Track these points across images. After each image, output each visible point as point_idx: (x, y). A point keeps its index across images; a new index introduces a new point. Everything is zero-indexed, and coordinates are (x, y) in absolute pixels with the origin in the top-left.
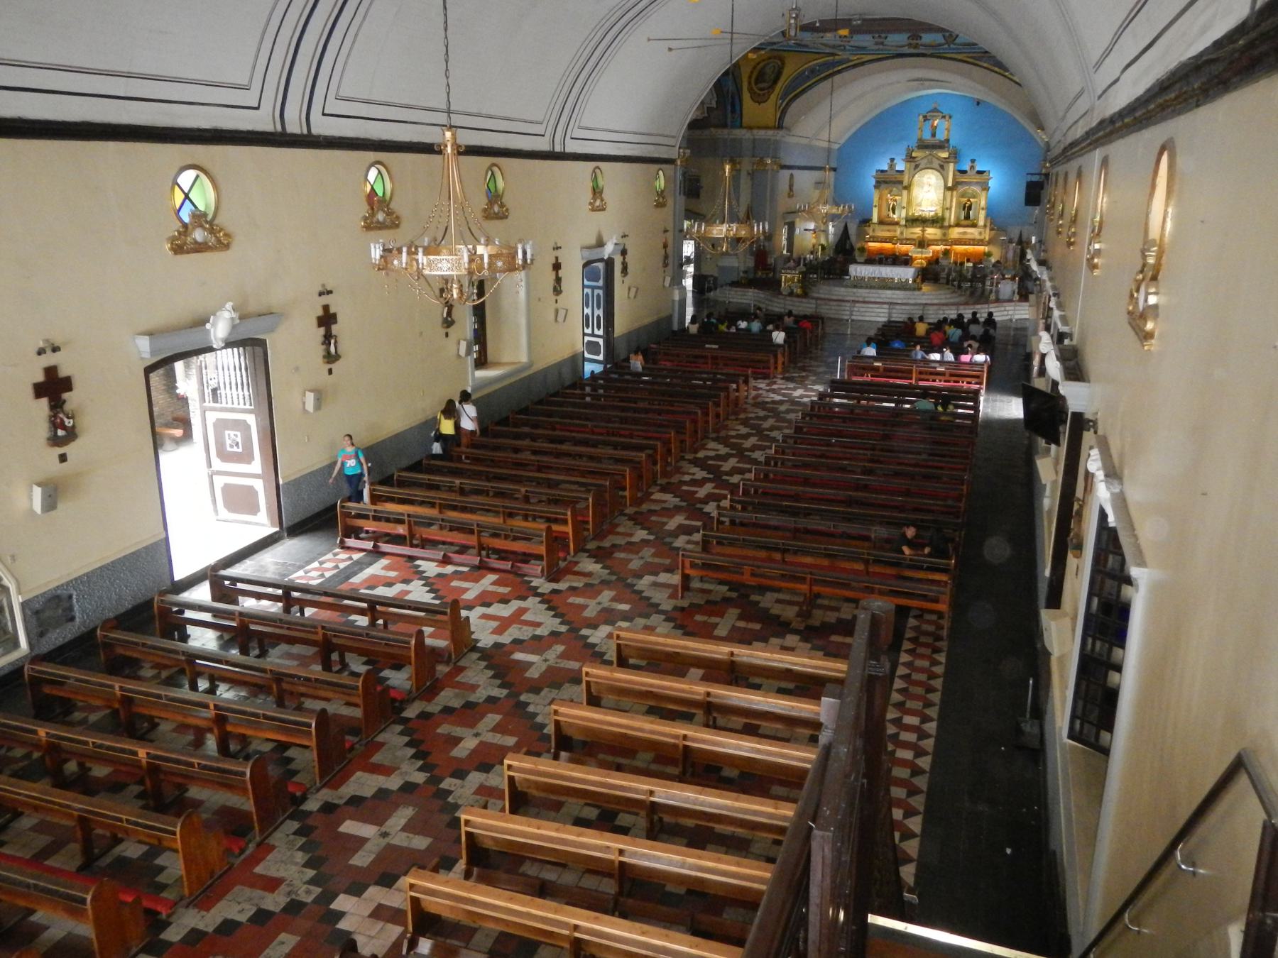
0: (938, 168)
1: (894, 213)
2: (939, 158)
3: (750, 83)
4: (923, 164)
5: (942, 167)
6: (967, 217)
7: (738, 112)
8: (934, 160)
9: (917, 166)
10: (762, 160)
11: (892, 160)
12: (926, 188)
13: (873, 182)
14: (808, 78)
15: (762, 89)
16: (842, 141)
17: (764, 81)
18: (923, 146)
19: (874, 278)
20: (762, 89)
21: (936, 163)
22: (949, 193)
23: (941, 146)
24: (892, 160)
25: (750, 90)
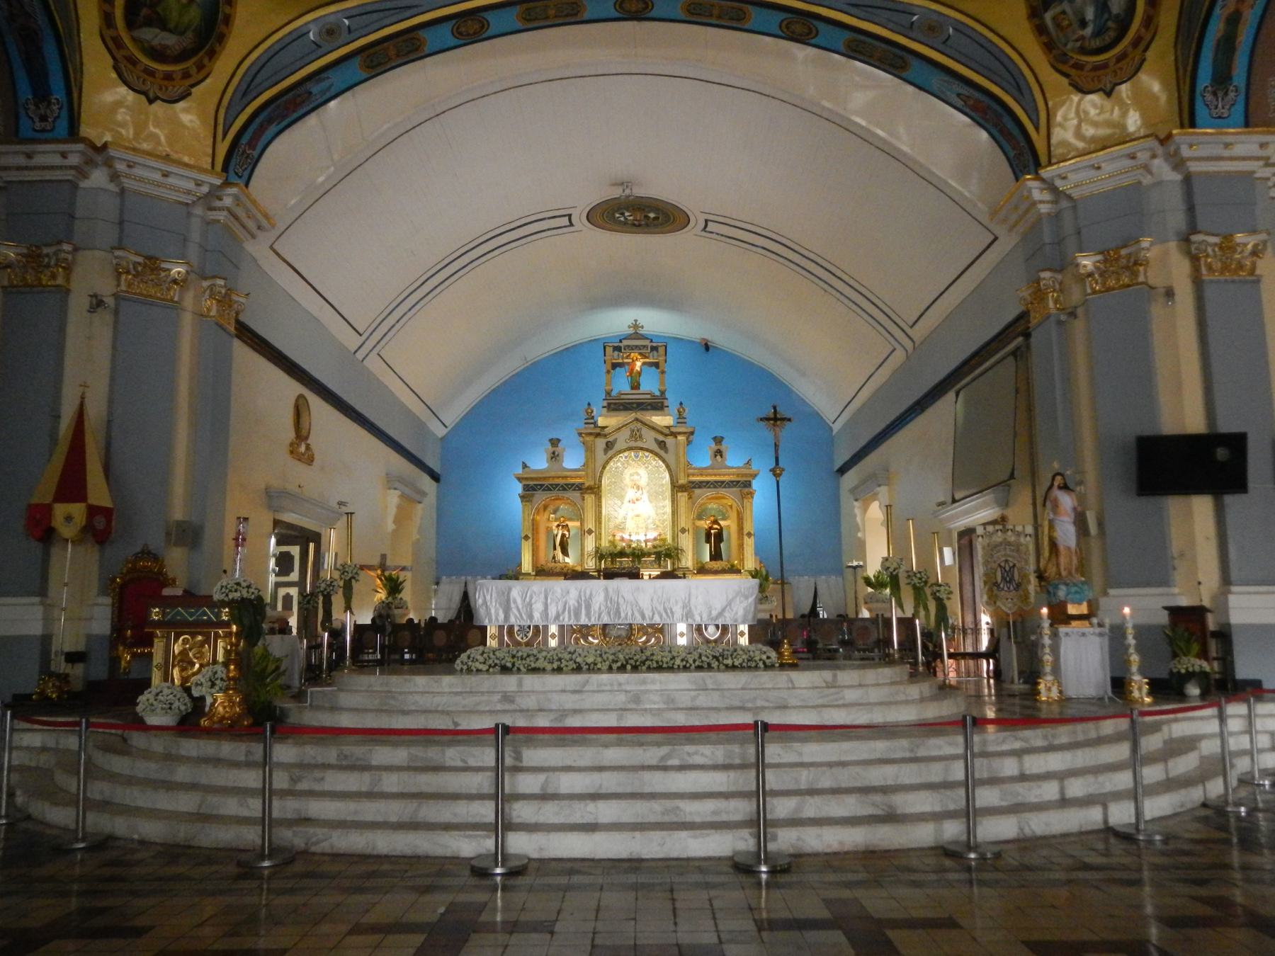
0: (655, 447)
1: (565, 552)
2: (653, 428)
3: (108, 19)
4: (622, 439)
5: (662, 445)
6: (716, 556)
7: (58, 94)
8: (645, 431)
9: (609, 446)
10: (152, 264)
11: (555, 442)
12: (631, 494)
13: (519, 488)
14: (317, 49)
15: (158, 54)
16: (452, 416)
17: (163, 25)
18: (616, 405)
19: (585, 631)
20: (158, 54)
21: (649, 438)
22: (682, 497)
23: (657, 405)
24: (555, 442)
25: (113, 44)
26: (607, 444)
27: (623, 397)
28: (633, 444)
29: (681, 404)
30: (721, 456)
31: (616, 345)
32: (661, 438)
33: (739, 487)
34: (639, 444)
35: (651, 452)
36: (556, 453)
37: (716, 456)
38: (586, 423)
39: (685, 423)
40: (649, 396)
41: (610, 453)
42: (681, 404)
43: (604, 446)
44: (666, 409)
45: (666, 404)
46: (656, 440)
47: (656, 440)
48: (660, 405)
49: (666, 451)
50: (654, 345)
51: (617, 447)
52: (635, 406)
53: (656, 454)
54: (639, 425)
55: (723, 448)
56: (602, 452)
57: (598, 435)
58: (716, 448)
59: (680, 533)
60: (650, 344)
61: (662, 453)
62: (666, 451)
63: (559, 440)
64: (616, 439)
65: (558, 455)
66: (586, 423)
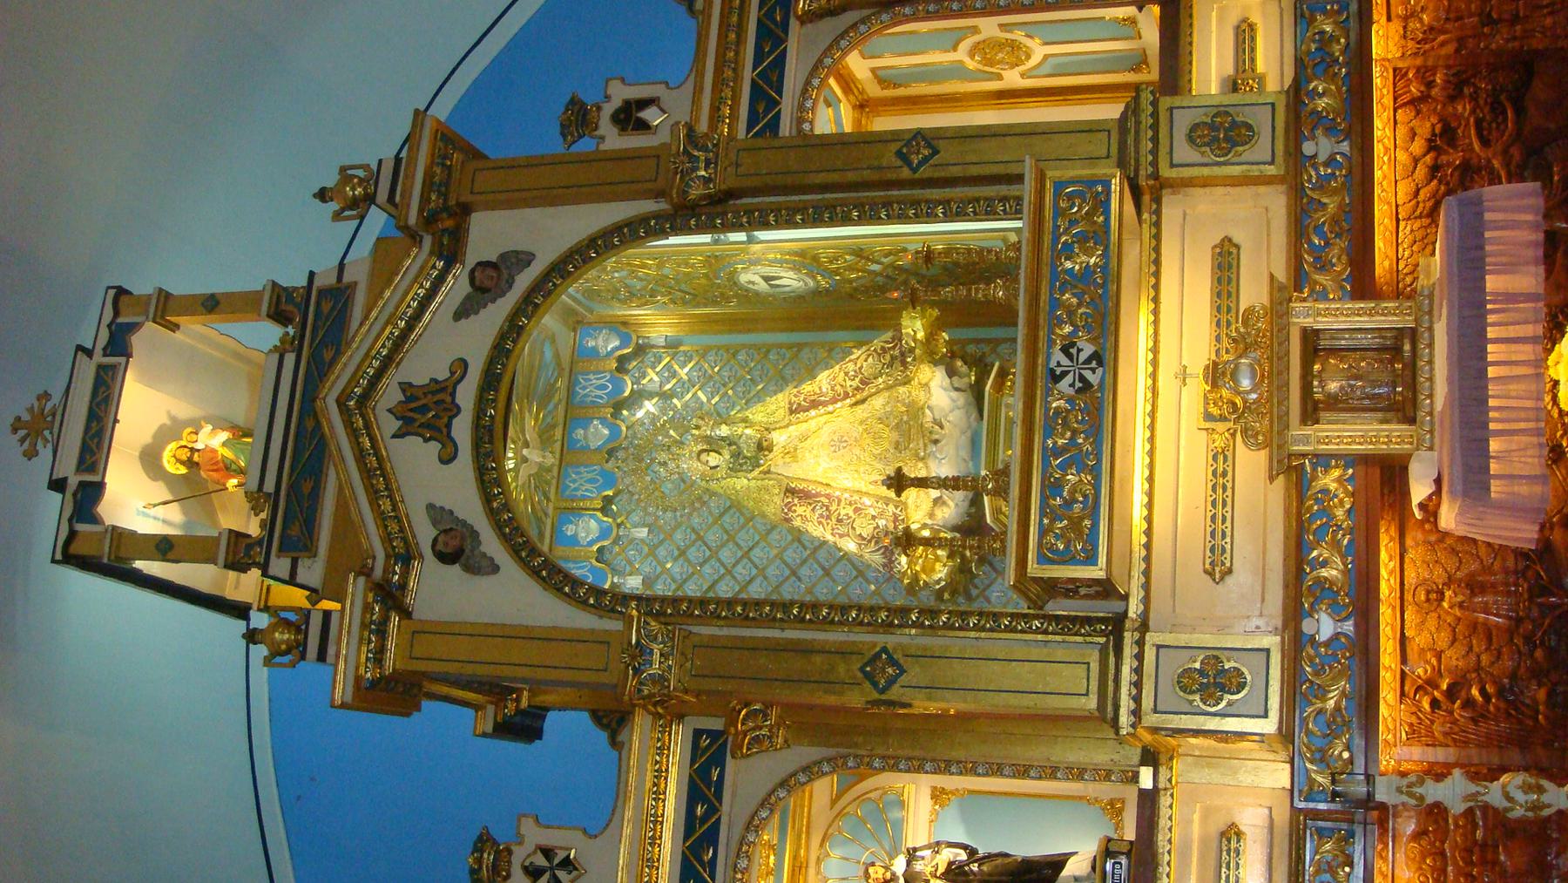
0: (496, 314)
26: (446, 558)
27: (269, 486)
28: (462, 429)
29: (323, 195)
30: (644, 103)
31: (68, 513)
32: (457, 286)
33: (785, 26)
34: (466, 395)
35: (513, 331)
36: (541, 861)
37: (643, 126)
38: (322, 657)
39: (398, 160)
40: (290, 359)
41: (491, 544)
42: (323, 195)
43: (456, 569)
44: (347, 278)
45: (331, 280)
46: (463, 312)
47: (463, 312)
48: (326, 307)
49: (523, 259)
50: (104, 335)
51: (470, 508)
52: (310, 424)
53: (530, 305)
54: (389, 394)
55: (620, 93)
56: (484, 582)
57: (391, 596)
58: (606, 127)
59: (924, 172)
60: (98, 357)
61: (524, 280)
62: (522, 259)
63: (484, 841)
64: (431, 507)
65: (547, 852)
66: (322, 657)
